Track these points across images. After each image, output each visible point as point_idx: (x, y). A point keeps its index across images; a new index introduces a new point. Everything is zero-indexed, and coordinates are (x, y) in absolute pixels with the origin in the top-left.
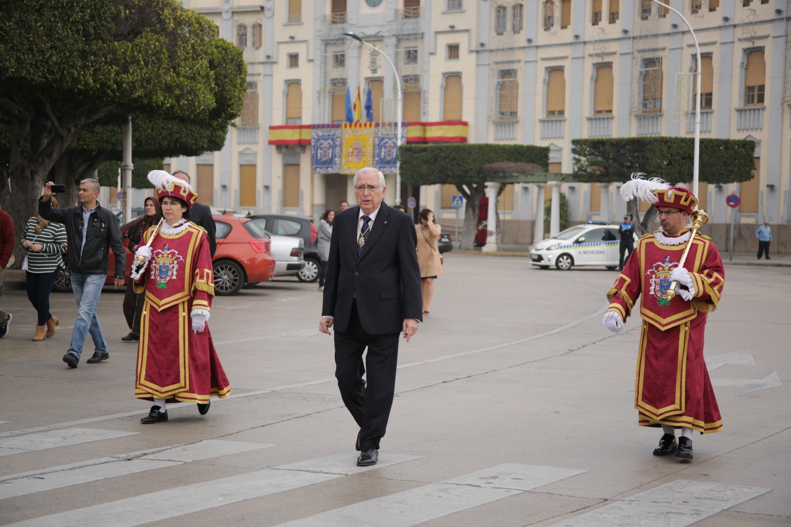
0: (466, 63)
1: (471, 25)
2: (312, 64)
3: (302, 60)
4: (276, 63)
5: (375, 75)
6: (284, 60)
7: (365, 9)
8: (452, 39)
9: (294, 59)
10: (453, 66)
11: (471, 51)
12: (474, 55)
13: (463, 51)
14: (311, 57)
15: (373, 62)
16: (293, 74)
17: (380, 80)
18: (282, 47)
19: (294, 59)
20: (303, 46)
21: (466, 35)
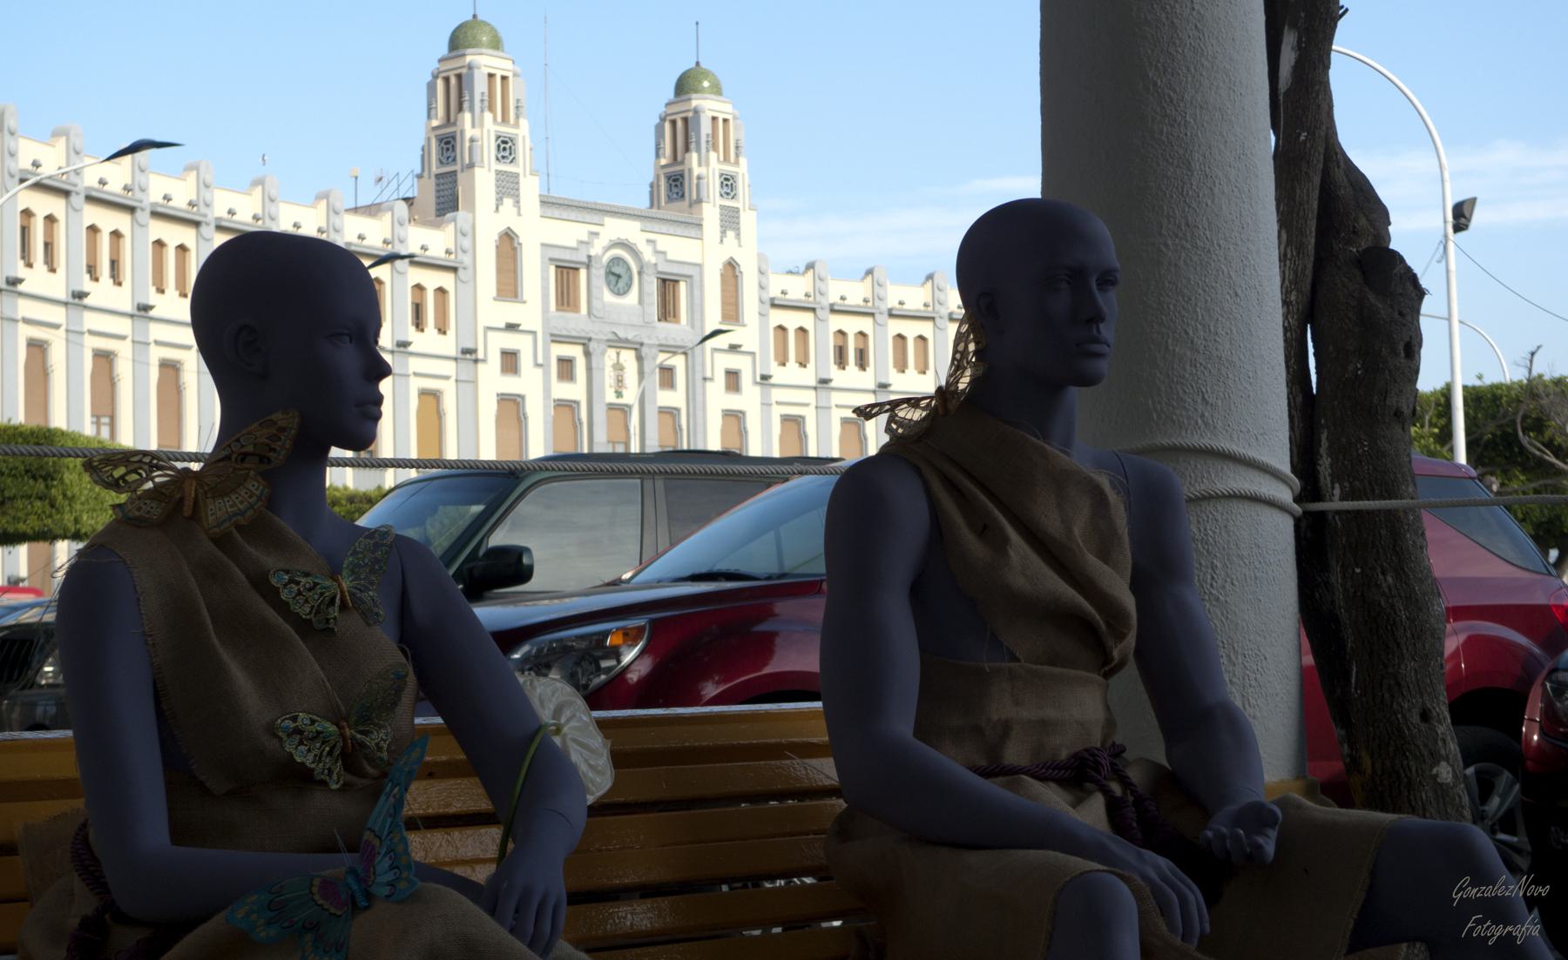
0: (748, 399)
1: (756, 349)
2: (540, 371)
3: (526, 361)
4: (484, 361)
5: (620, 401)
6: (495, 360)
7: (608, 297)
8: (733, 362)
9: (510, 361)
10: (734, 402)
11: (756, 383)
12: (758, 389)
13: (746, 380)
14: (540, 361)
15: (620, 380)
16: (511, 385)
17: (624, 410)
18: (491, 334)
19: (510, 361)
20: (530, 338)
21: (749, 359)
